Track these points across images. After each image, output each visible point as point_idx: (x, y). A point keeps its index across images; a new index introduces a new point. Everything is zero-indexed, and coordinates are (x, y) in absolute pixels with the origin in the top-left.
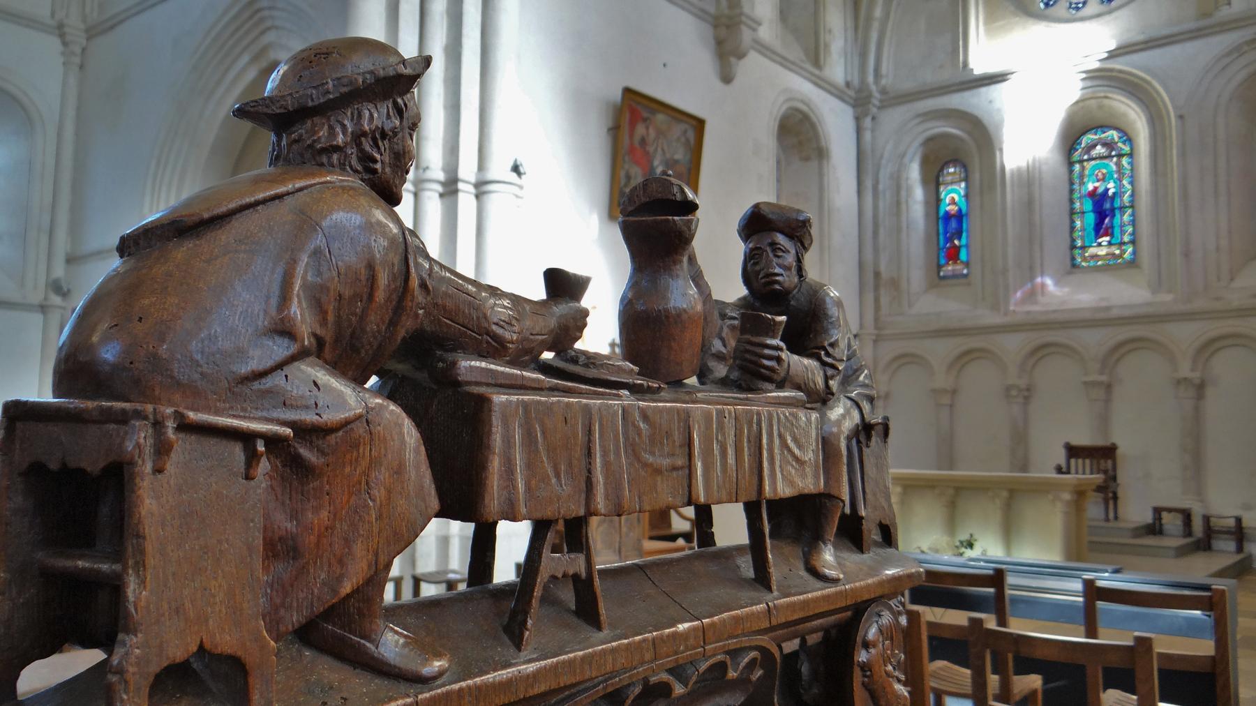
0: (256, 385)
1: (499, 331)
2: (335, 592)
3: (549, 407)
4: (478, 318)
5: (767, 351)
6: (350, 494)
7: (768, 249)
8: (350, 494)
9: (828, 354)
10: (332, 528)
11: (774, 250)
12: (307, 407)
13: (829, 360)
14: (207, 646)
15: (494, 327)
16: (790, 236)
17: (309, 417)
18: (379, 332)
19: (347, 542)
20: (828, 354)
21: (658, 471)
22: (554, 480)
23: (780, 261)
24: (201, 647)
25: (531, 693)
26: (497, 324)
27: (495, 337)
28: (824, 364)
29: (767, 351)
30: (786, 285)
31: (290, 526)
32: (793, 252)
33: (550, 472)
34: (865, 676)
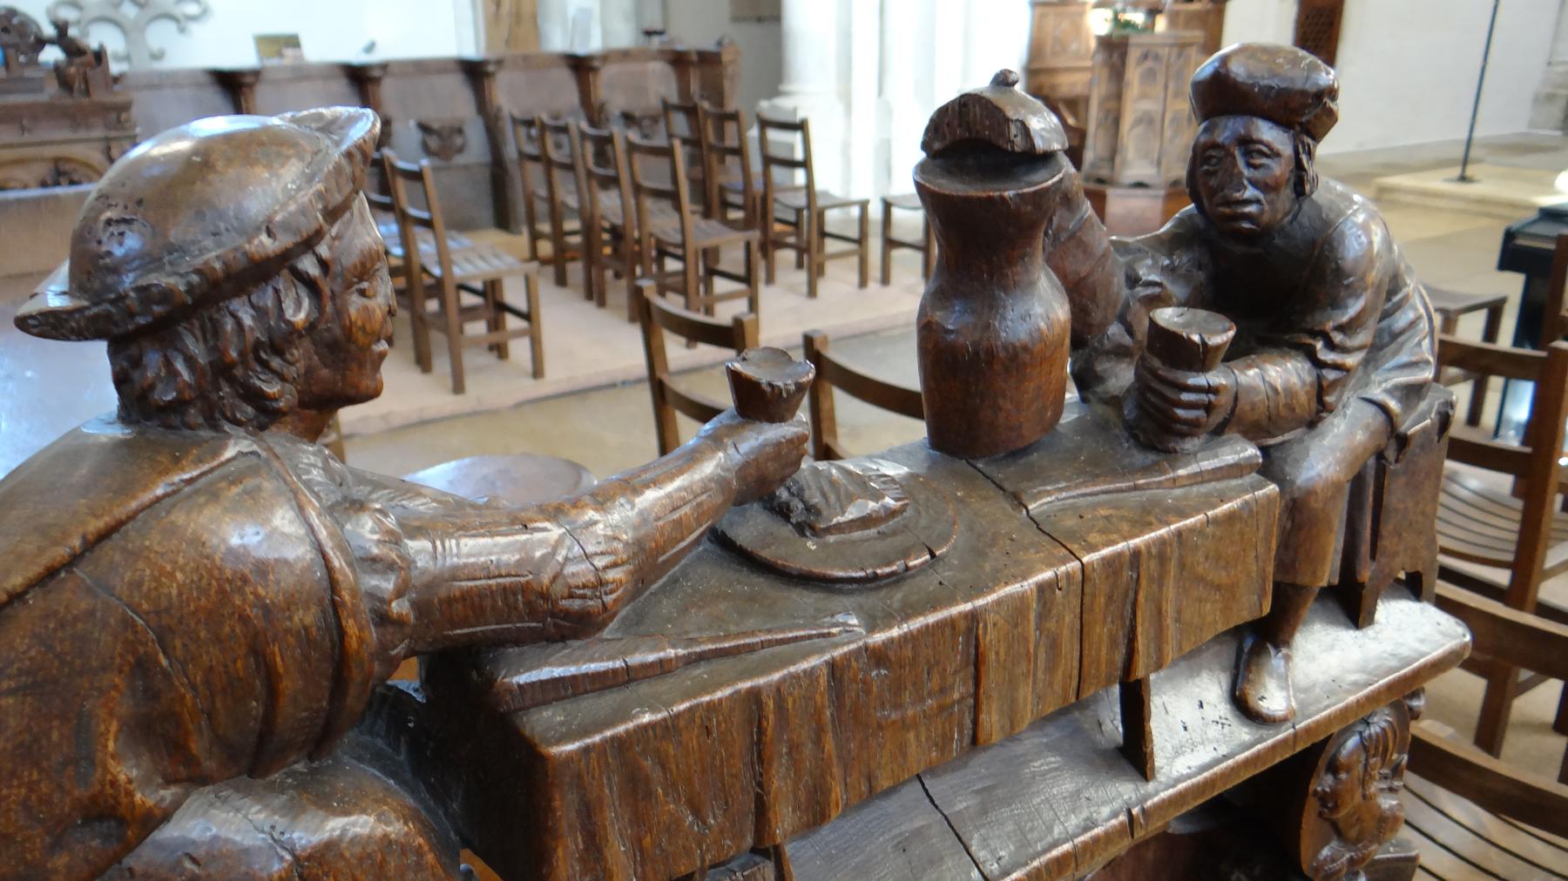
1: (576, 604)
5: (1185, 397)
7: (1237, 153)
9: (1331, 346)
11: (1248, 154)
13: (1329, 357)
15: (564, 603)
23: (1257, 174)
26: (571, 596)
27: (567, 614)
28: (1319, 364)
29: (1185, 397)
30: (1266, 218)
32: (1286, 149)
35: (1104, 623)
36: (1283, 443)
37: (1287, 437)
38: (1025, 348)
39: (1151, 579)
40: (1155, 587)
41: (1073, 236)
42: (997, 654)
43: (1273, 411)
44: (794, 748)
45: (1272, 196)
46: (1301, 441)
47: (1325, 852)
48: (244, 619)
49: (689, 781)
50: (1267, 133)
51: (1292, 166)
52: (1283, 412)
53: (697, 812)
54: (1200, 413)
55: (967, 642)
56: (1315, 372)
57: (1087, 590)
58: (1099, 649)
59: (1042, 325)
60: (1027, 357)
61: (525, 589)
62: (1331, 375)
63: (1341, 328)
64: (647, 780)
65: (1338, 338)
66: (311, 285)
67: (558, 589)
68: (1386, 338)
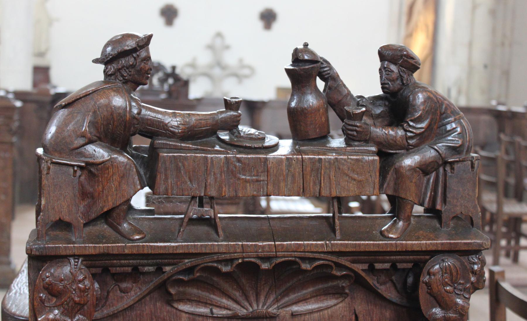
0: (76, 151)
2: (102, 209)
3: (186, 158)
4: (163, 126)
6: (107, 183)
8: (107, 183)
10: (103, 192)
12: (91, 157)
14: (62, 219)
16: (395, 64)
17: (91, 160)
18: (121, 133)
19: (107, 196)
20: (410, 126)
21: (246, 181)
22: (189, 183)
24: (60, 219)
25: (175, 252)
26: (172, 127)
27: (171, 131)
28: (406, 131)
30: (391, 89)
31: (91, 190)
33: (187, 180)
34: (428, 289)
35: (311, 176)
36: (396, 153)
37: (397, 151)
38: (305, 108)
39: (326, 168)
40: (328, 171)
41: (336, 88)
42: (273, 171)
43: (386, 140)
44: (214, 174)
45: (393, 83)
46: (403, 155)
47: (434, 310)
48: (111, 108)
49: (189, 172)
50: (393, 67)
51: (398, 75)
52: (391, 141)
53: (191, 181)
54: (355, 133)
55: (264, 165)
56: (404, 133)
57: (304, 164)
58: (310, 183)
59: (311, 104)
60: (306, 111)
61: (163, 122)
62: (409, 134)
63: (412, 121)
64: (180, 168)
65: (411, 124)
66: (135, 58)
67: (169, 125)
68: (444, 132)
